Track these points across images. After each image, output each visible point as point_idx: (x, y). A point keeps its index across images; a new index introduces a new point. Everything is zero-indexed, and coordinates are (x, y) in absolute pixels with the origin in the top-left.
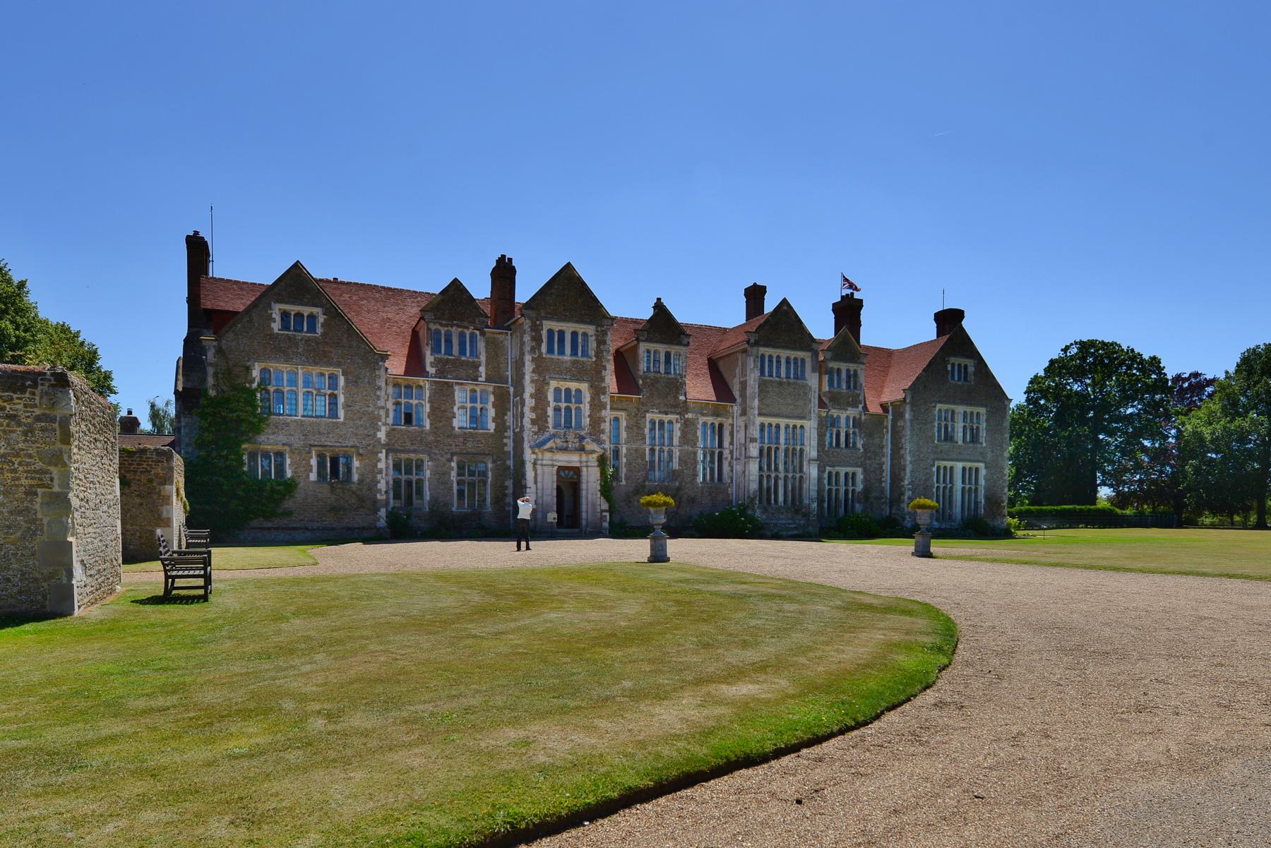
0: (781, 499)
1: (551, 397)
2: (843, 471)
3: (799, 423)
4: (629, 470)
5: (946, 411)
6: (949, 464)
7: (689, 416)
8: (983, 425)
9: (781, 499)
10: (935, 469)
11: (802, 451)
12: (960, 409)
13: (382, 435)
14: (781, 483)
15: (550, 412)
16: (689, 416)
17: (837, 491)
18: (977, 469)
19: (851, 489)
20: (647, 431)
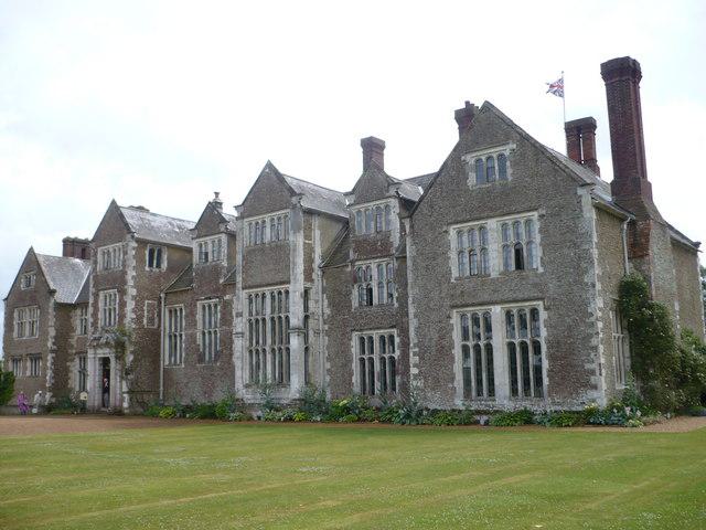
0: (269, 376)
1: (101, 305)
2: (376, 335)
3: (282, 288)
4: (187, 354)
5: (471, 230)
6: (480, 311)
7: (227, 297)
8: (537, 238)
9: (269, 376)
10: (455, 320)
11: (287, 317)
12: (493, 224)
13: (50, 344)
14: (269, 357)
15: (100, 315)
16: (227, 297)
17: (371, 360)
18: (534, 312)
19: (386, 356)
20: (199, 317)
